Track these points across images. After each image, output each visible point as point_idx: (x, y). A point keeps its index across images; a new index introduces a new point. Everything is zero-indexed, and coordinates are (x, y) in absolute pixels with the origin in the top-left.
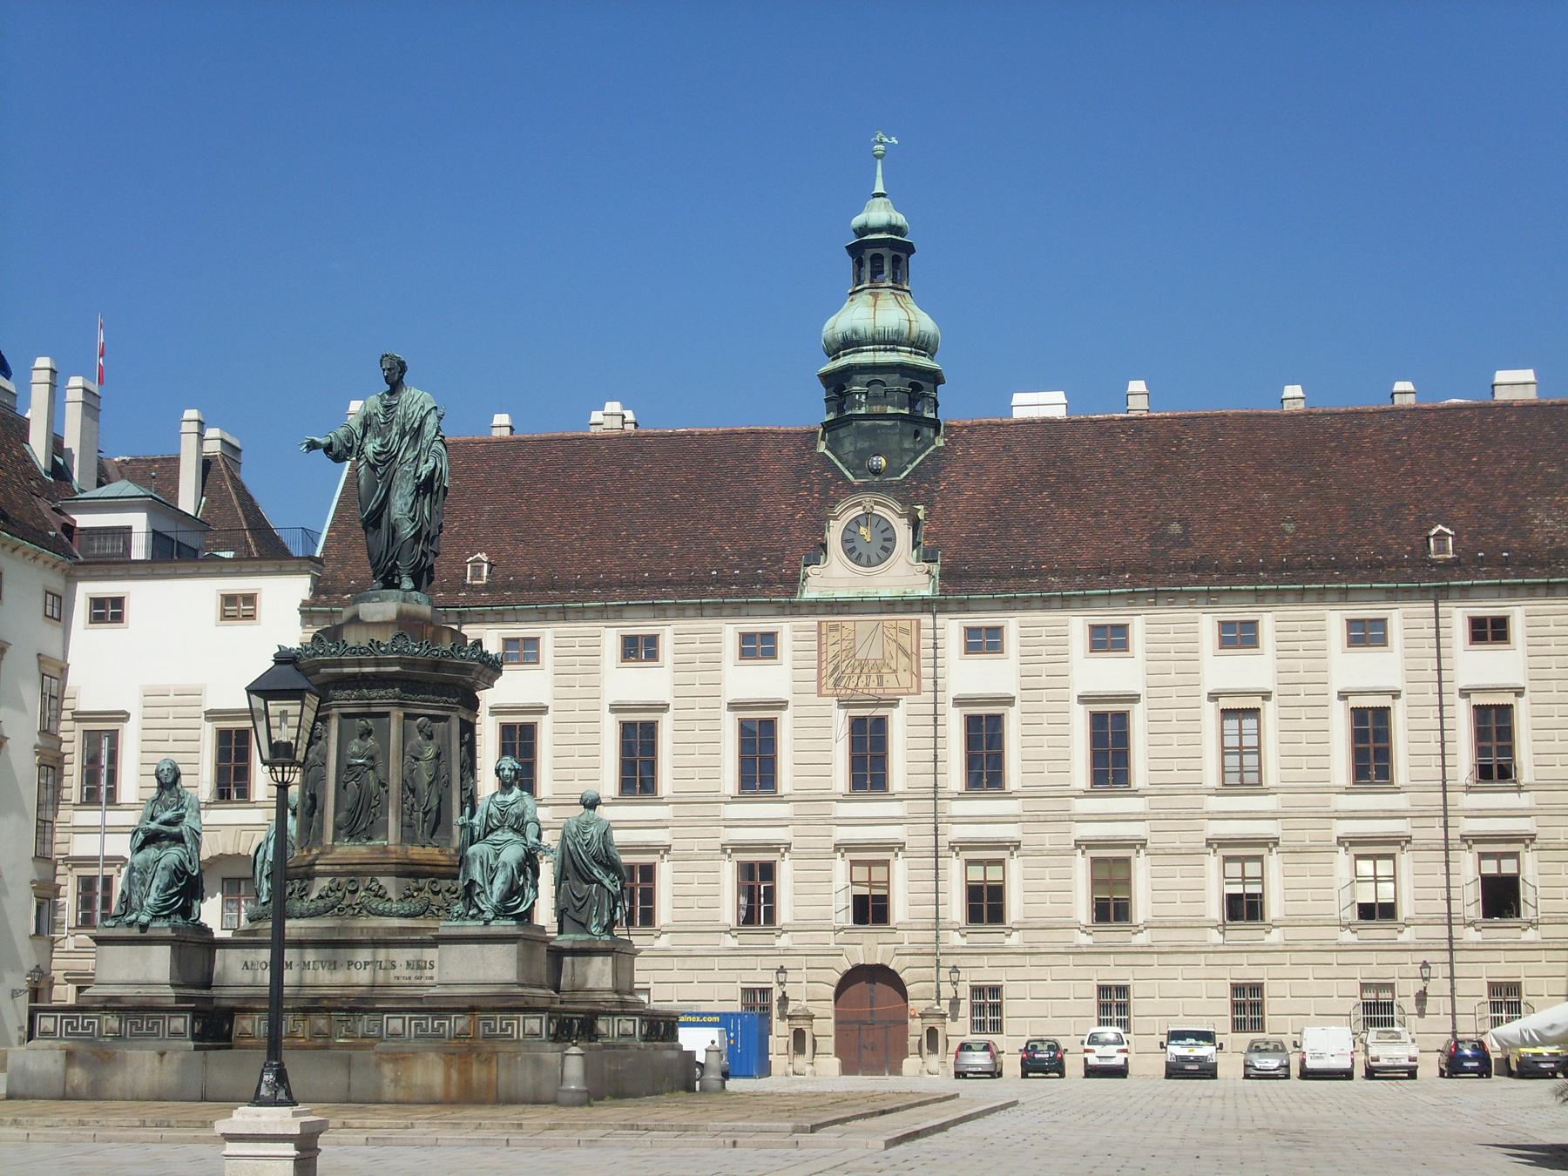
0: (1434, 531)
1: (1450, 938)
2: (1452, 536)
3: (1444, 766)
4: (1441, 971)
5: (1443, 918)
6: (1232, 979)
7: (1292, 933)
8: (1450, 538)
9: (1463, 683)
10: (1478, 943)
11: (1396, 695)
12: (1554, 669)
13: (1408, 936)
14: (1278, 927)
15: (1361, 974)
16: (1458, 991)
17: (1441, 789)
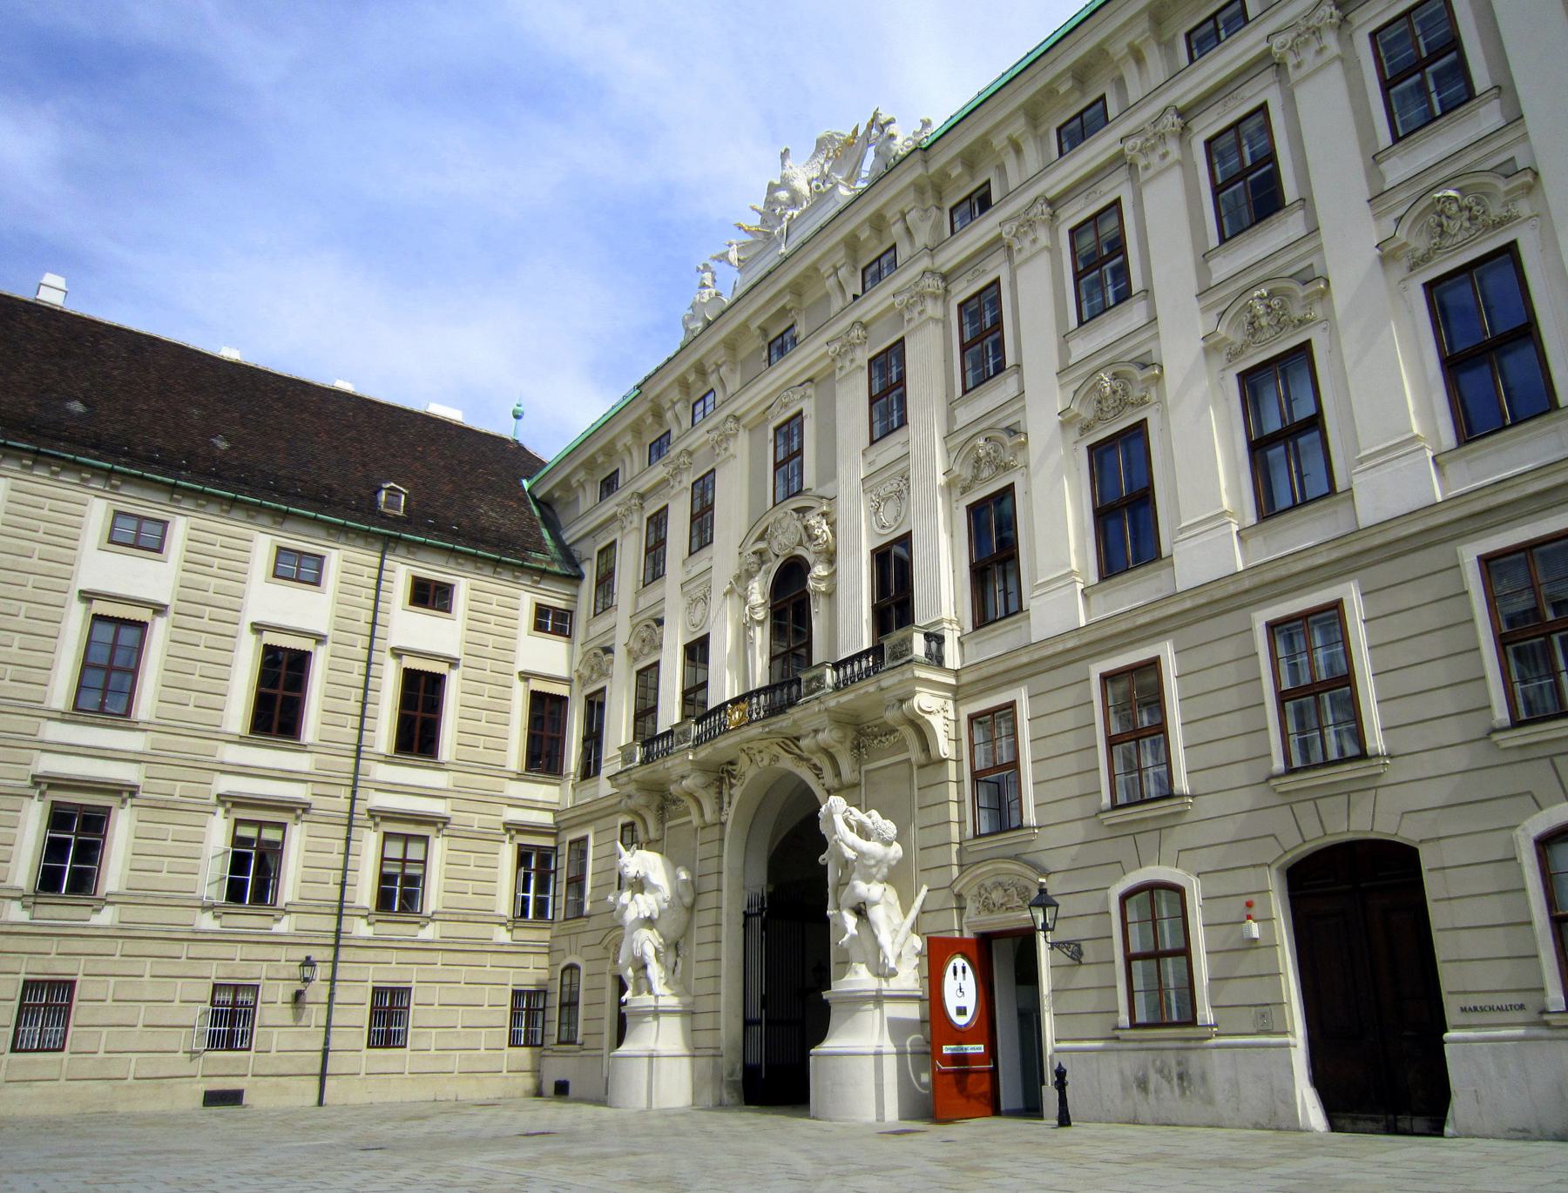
0: (388, 486)
1: (338, 931)
2: (406, 494)
3: (361, 729)
4: (322, 971)
5: (331, 907)
6: (27, 973)
7: (133, 914)
8: (403, 497)
9: (397, 641)
10: (369, 939)
11: (320, 639)
12: (490, 648)
13: (285, 926)
14: (113, 903)
15: (216, 972)
16: (337, 999)
17: (354, 754)
